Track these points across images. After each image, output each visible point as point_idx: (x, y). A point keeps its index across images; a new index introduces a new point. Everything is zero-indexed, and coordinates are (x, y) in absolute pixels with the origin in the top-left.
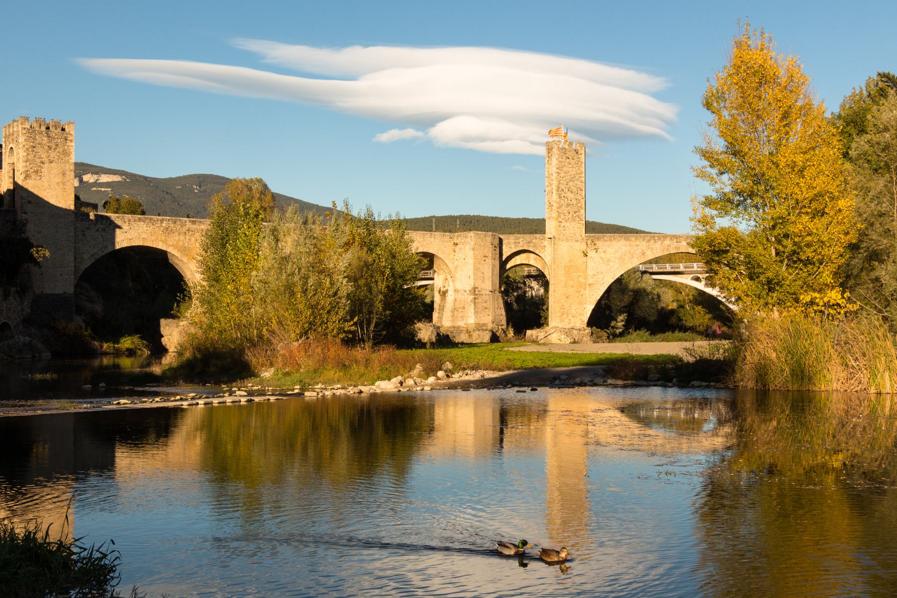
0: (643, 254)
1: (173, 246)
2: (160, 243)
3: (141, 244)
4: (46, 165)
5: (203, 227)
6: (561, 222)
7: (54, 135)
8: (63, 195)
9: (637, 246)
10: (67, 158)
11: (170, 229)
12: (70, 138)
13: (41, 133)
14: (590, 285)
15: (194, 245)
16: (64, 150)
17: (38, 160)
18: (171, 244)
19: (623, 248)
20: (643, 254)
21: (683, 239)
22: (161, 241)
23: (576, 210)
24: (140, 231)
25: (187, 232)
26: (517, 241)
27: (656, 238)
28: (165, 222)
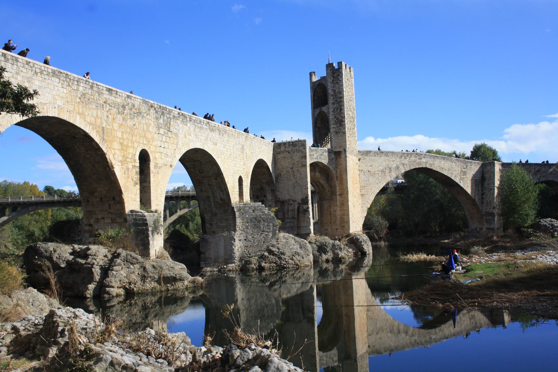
0: (398, 168)
1: (90, 124)
3: (56, 116)
5: (119, 100)
9: (393, 161)
11: (87, 96)
14: (362, 195)
15: (111, 127)
18: (89, 121)
19: (384, 162)
20: (398, 168)
21: (422, 156)
22: (79, 113)
24: (54, 93)
25: (105, 105)
26: (312, 153)
27: (406, 155)
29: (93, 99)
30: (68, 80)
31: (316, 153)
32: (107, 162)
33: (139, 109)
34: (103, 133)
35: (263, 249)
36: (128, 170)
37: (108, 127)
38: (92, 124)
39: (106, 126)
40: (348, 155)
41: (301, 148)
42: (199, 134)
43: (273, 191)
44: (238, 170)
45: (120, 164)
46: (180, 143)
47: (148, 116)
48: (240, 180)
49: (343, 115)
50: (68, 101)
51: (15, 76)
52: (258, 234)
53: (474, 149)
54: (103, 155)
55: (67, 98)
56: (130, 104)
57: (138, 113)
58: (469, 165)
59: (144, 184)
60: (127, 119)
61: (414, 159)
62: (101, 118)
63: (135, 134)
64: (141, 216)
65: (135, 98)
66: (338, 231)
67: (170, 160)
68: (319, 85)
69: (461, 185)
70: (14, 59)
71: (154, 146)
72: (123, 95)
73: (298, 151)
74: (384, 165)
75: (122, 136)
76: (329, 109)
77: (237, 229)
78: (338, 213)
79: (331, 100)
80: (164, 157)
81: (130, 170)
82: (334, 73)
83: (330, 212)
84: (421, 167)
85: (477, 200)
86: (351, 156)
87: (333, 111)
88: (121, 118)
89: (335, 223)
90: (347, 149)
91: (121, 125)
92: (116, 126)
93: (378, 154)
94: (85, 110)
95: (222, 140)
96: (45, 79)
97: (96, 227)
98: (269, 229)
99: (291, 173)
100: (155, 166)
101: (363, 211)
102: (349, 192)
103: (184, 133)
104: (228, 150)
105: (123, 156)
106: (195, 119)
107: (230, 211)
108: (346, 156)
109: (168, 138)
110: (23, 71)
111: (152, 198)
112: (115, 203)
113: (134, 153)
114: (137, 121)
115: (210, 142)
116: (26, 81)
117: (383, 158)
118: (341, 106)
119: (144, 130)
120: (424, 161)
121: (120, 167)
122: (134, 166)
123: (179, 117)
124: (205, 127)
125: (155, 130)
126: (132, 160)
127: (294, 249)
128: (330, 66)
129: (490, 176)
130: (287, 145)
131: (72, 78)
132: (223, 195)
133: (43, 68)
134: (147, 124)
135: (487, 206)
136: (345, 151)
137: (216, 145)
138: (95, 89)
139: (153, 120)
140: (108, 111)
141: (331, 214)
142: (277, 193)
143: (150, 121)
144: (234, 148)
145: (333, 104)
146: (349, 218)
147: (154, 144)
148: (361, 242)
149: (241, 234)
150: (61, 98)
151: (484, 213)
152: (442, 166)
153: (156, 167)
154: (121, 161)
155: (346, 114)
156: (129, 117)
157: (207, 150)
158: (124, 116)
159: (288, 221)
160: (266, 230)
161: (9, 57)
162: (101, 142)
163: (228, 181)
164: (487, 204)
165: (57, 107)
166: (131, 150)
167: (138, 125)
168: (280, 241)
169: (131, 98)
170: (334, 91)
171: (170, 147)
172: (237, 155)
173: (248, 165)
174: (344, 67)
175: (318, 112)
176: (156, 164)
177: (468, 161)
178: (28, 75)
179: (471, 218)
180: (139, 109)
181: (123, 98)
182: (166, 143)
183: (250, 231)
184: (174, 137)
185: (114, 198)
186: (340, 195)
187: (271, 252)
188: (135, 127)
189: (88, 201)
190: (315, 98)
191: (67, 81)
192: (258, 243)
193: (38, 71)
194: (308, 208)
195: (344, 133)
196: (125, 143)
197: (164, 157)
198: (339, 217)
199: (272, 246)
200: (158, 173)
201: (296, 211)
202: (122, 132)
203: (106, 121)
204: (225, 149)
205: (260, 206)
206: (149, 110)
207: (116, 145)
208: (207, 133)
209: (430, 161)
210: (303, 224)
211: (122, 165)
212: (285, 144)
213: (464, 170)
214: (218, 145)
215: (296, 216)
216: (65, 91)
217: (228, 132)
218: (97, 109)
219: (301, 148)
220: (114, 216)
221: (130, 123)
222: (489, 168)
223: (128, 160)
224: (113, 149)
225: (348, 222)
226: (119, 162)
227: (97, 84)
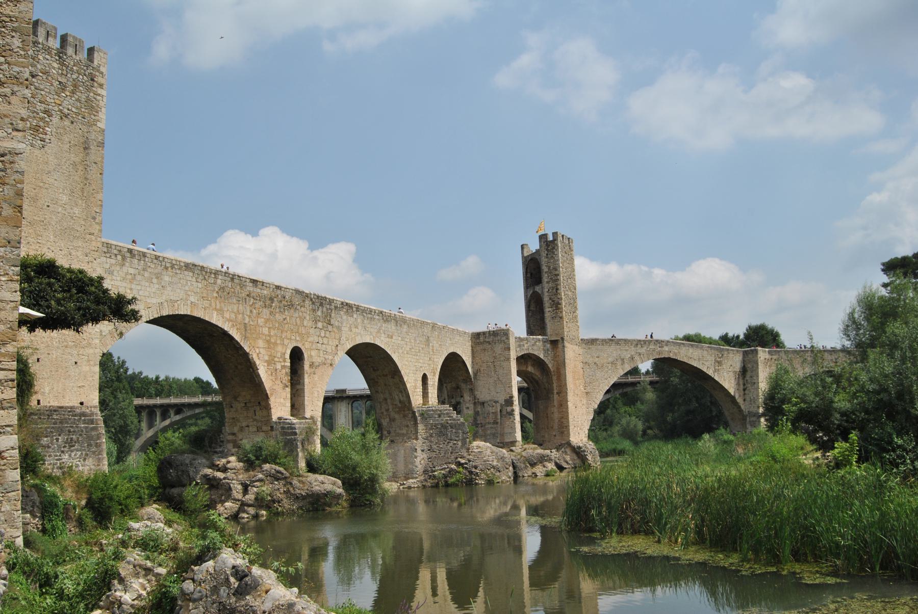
1: (229, 320)
2: (215, 313)
3: (189, 313)
4: (56, 120)
5: (265, 292)
6: (567, 322)
7: (72, 63)
8: (83, 193)
9: (626, 350)
10: (92, 116)
11: (227, 290)
12: (99, 79)
13: (48, 50)
14: (587, 393)
16: (88, 100)
17: (40, 107)
18: (228, 317)
21: (664, 343)
23: (573, 310)
24: (187, 288)
25: (248, 298)
26: (522, 343)
27: (642, 343)
28: (220, 277)
29: (234, 292)
30: (204, 273)
31: (527, 343)
32: (250, 362)
33: (291, 301)
34: (246, 330)
35: (450, 461)
36: (276, 370)
37: (251, 323)
38: (231, 321)
39: (249, 322)
40: (566, 344)
41: (504, 338)
42: (369, 326)
43: (472, 390)
44: (421, 367)
45: (266, 364)
46: (343, 338)
47: (302, 308)
48: (425, 378)
49: (559, 297)
50: (203, 297)
51: (142, 272)
52: (444, 444)
53: (747, 330)
54: (246, 354)
55: (202, 293)
56: (280, 296)
57: (289, 305)
58: (726, 353)
59: (298, 387)
60: (276, 313)
61: (653, 347)
62: (243, 314)
63: (286, 329)
64: (289, 424)
65: (285, 288)
66: (557, 437)
67: (330, 357)
68: (531, 259)
69: (716, 378)
70: (141, 255)
71: (310, 342)
72: (271, 286)
73: (501, 341)
74: (615, 355)
75: (269, 332)
76: (545, 289)
77: (420, 437)
78: (556, 416)
79: (545, 278)
80: (321, 355)
81: (278, 371)
82: (548, 245)
83: (547, 414)
84: (663, 357)
85: (737, 397)
86: (571, 346)
87: (547, 292)
88: (268, 313)
89: (552, 428)
90: (565, 338)
91: (267, 321)
92: (261, 321)
93: (607, 343)
94: (223, 306)
95: (399, 332)
96: (176, 273)
97: (240, 437)
98: (458, 437)
99: (493, 368)
100: (310, 365)
101: (588, 413)
102: (568, 389)
103: (348, 326)
104: (408, 343)
105: (271, 355)
106: (363, 308)
107: (410, 416)
108: (564, 346)
109: (328, 332)
110: (152, 266)
111: (306, 403)
112: (260, 409)
113: (284, 352)
114: (288, 315)
115: (383, 335)
116: (154, 277)
117: (613, 347)
118: (557, 285)
119: (296, 325)
120: (667, 349)
121: (266, 367)
122: (283, 367)
123: (343, 307)
124: (377, 317)
125: (310, 324)
126: (281, 360)
127: (489, 461)
128: (543, 237)
129: (753, 367)
130: (487, 335)
131: (208, 271)
132: (403, 396)
133: (174, 262)
134: (300, 317)
135: (751, 404)
136: (563, 339)
137: (392, 337)
138: (236, 281)
139: (308, 312)
140: (251, 306)
141: (548, 417)
142: (476, 393)
143: (305, 314)
144: (415, 340)
145: (548, 282)
146: (568, 422)
147: (310, 339)
148: (584, 451)
149: (423, 443)
150: (195, 293)
151: (747, 413)
152: (689, 354)
153: (312, 365)
154: (266, 361)
155: (563, 294)
156: (278, 310)
157: (379, 344)
158: (272, 310)
159: (490, 426)
160: (453, 437)
161: (136, 253)
162: (243, 342)
163: (408, 379)
164: (751, 401)
165: (189, 302)
166: (280, 348)
167: (290, 319)
168: (472, 452)
169: (281, 289)
170: (549, 267)
171: (330, 342)
172: (421, 349)
173: (436, 360)
174: (560, 238)
175: (531, 292)
176: (313, 363)
177: (723, 349)
178: (156, 271)
179: (732, 419)
180: (291, 301)
181: (271, 290)
182: (325, 339)
183: (434, 439)
184: (336, 331)
185: (259, 403)
186: (557, 393)
187: (459, 464)
188: (285, 322)
189: (232, 407)
190: (529, 275)
191: (202, 274)
192: (445, 453)
193: (168, 265)
194: (513, 410)
195: (561, 318)
196: (273, 341)
197: (321, 355)
198: (557, 421)
199: (461, 458)
200: (314, 374)
201: (499, 413)
202: (269, 328)
203: (250, 317)
204: (404, 342)
205: (446, 410)
206: (304, 301)
207: (261, 343)
208: (379, 325)
209: (675, 349)
210: (507, 430)
211: (268, 366)
212: (484, 333)
213: (719, 360)
214: (394, 337)
215: (499, 421)
216: (200, 285)
217: (408, 322)
218: (238, 304)
219: (504, 338)
220: (259, 424)
221: (279, 317)
222: (750, 356)
223: (276, 359)
224: (258, 348)
225: (567, 427)
226: (265, 362)
227: (238, 276)
